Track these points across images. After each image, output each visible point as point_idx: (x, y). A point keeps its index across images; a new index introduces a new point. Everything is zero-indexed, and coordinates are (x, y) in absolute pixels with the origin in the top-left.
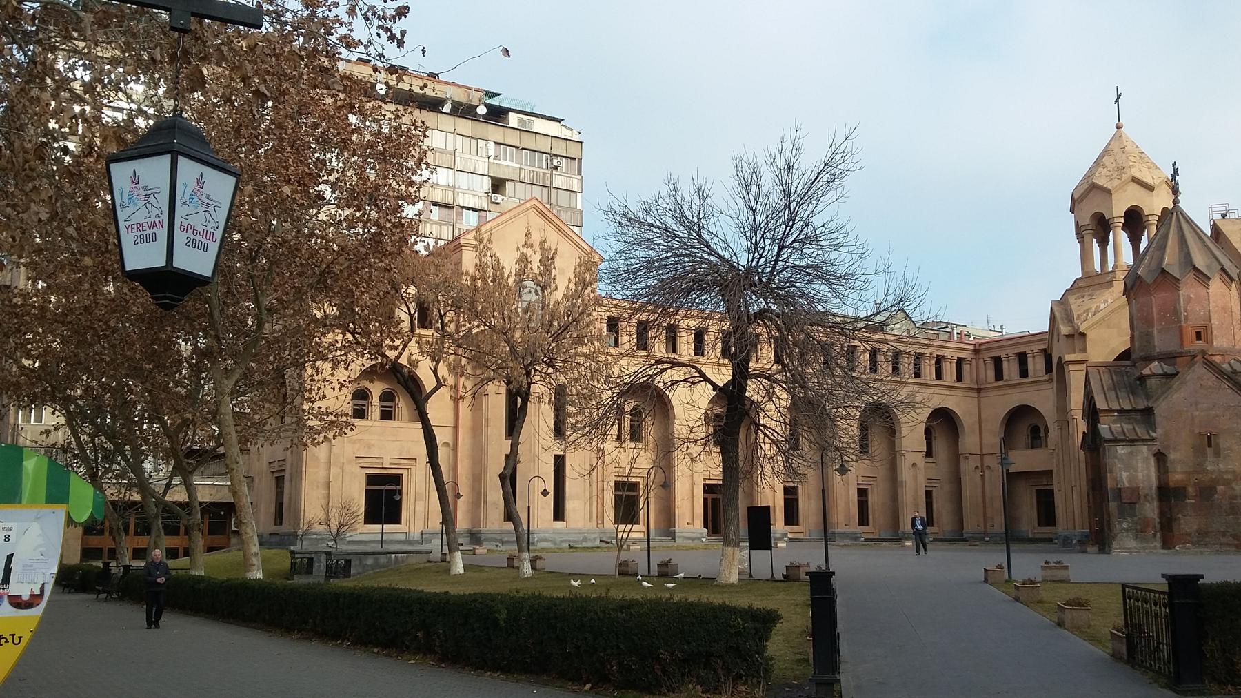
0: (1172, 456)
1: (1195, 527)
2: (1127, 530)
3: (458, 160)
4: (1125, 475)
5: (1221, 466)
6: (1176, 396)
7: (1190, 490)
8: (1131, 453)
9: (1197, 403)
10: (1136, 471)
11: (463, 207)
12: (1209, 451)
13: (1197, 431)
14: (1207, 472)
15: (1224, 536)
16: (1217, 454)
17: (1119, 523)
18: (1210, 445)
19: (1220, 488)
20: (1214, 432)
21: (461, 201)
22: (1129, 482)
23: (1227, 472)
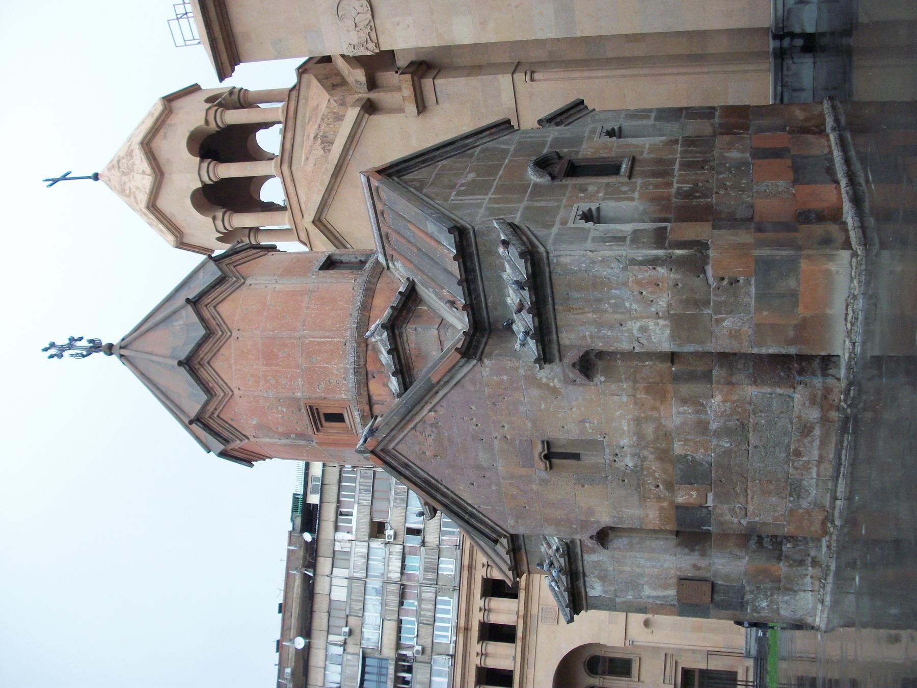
0: (605, 519)
1: (774, 499)
2: (772, 602)
3: (356, 575)
4: (648, 591)
5: (625, 441)
6: (465, 496)
7: (680, 500)
8: (603, 578)
9: (479, 467)
10: (642, 575)
11: (402, 573)
12: (589, 459)
13: (544, 475)
14: (638, 471)
15: (798, 454)
16: (595, 445)
17: (756, 609)
18: (576, 457)
19: (678, 448)
20: (539, 448)
21: (395, 575)
22: (665, 586)
23: (640, 435)
